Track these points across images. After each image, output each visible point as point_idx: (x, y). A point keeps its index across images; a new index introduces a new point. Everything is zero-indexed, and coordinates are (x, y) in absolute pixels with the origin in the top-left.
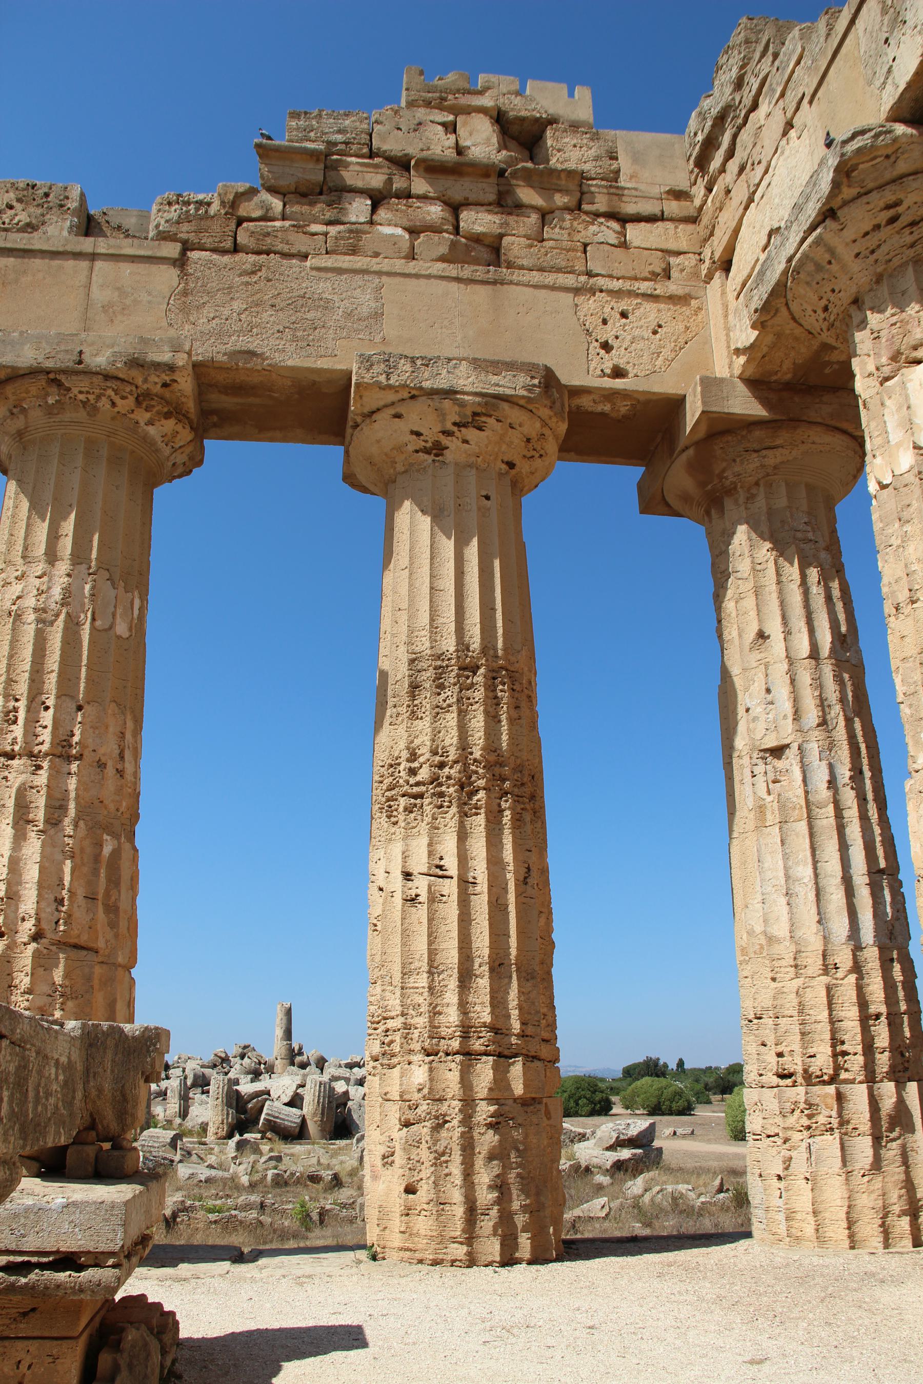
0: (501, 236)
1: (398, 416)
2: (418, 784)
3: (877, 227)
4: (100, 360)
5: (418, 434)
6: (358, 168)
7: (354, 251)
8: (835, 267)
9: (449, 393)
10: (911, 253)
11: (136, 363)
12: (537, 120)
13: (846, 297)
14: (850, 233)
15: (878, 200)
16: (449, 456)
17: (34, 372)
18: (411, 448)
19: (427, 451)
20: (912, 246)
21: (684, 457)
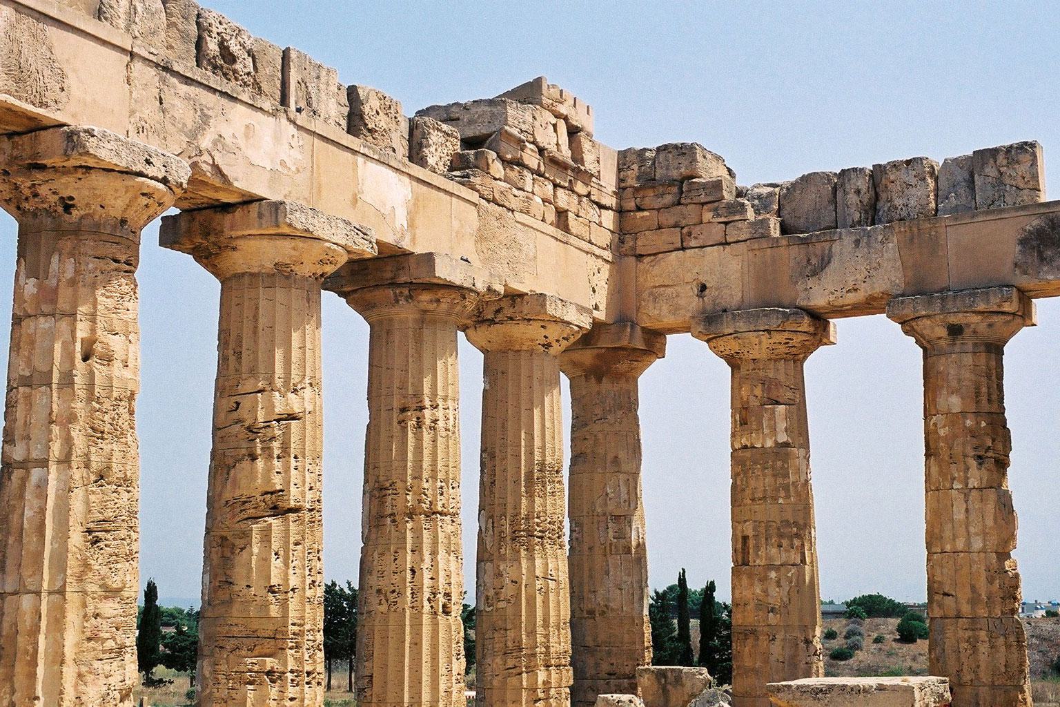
0: (567, 211)
1: (542, 327)
2: (540, 531)
3: (780, 343)
4: (481, 287)
5: (545, 337)
6: (529, 152)
7: (528, 213)
8: (757, 347)
9: (569, 323)
10: (785, 356)
11: (489, 289)
12: (577, 127)
13: (751, 357)
14: (770, 341)
15: (786, 335)
16: (552, 351)
17: (460, 288)
18: (538, 342)
19: (543, 345)
20: (787, 354)
21: (596, 351)
